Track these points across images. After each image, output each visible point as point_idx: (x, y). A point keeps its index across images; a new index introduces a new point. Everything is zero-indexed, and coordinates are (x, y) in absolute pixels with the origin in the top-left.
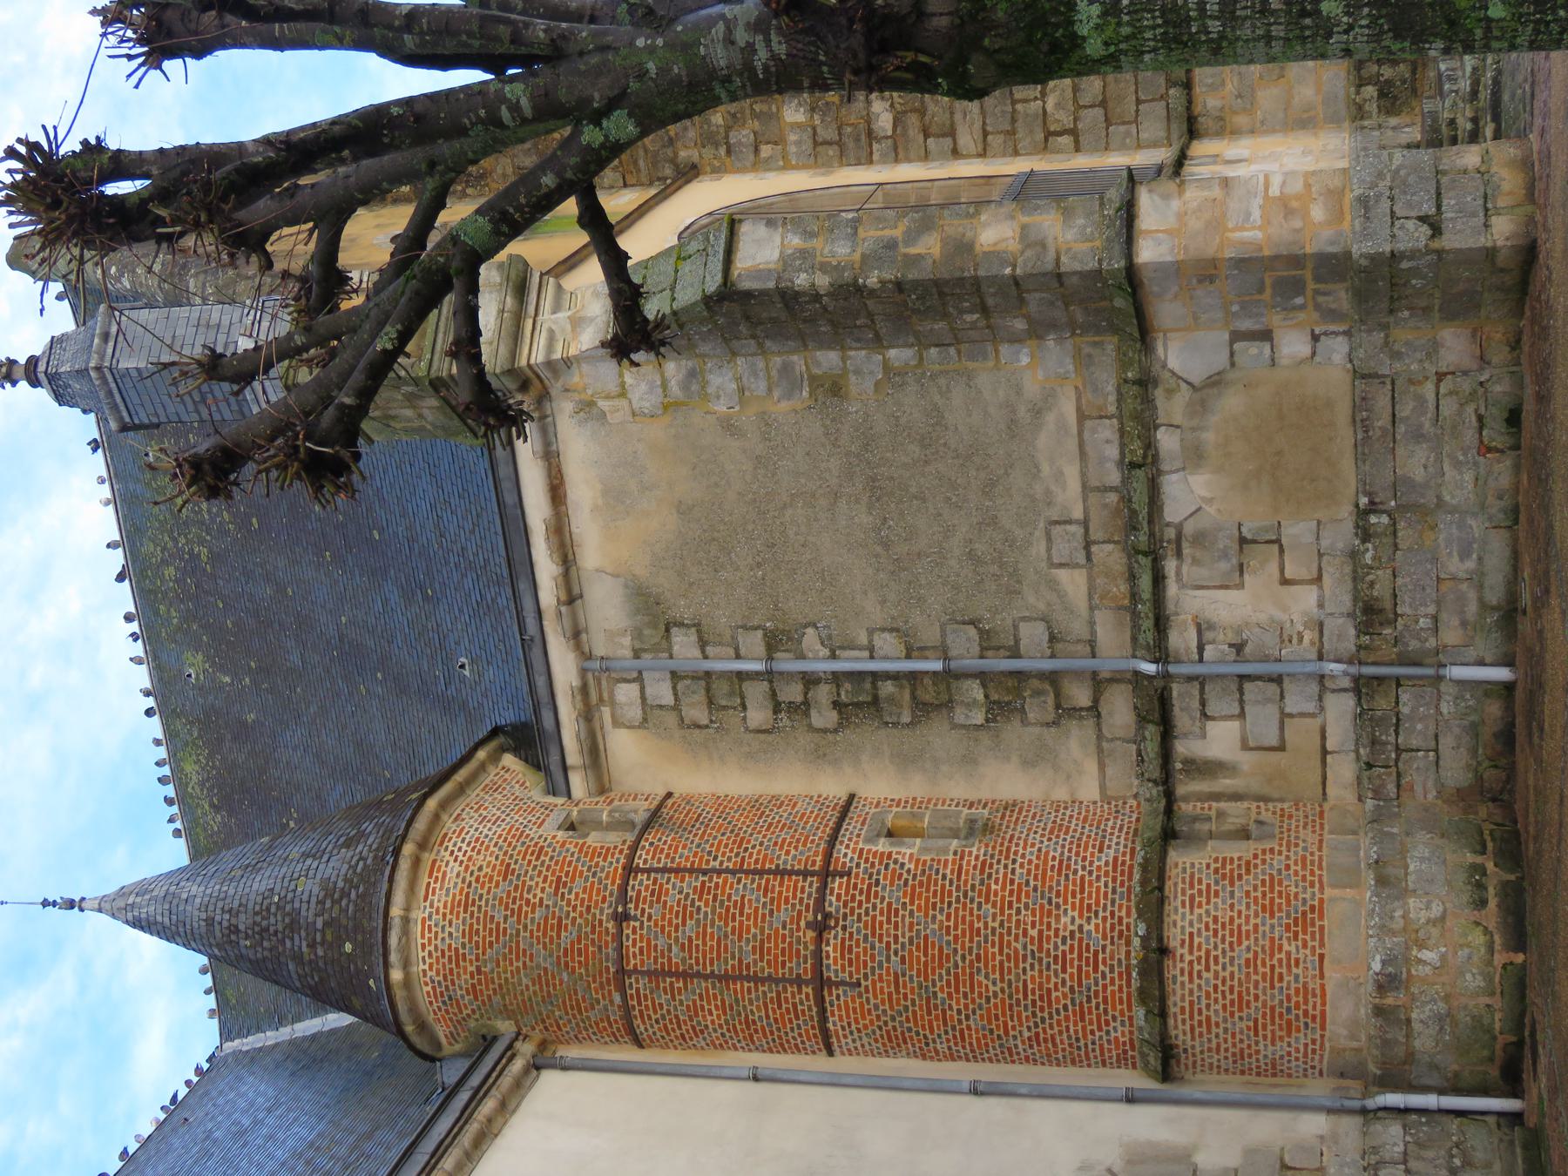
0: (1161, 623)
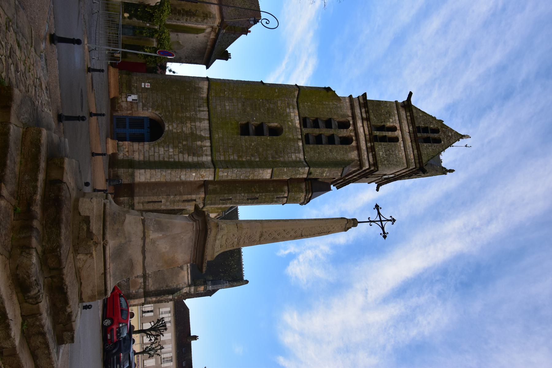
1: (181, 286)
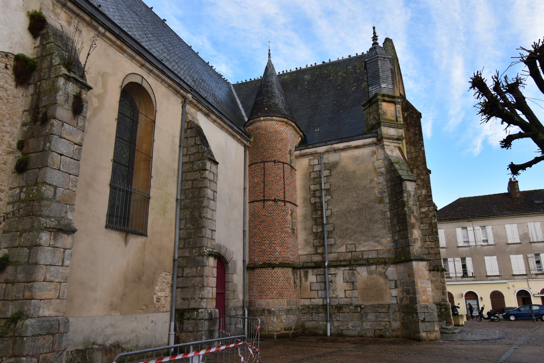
0: (336, 267)
1: (380, 164)
